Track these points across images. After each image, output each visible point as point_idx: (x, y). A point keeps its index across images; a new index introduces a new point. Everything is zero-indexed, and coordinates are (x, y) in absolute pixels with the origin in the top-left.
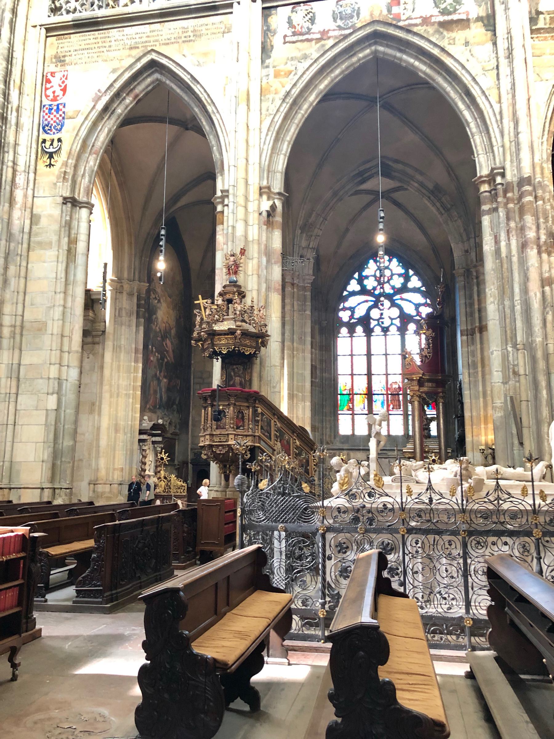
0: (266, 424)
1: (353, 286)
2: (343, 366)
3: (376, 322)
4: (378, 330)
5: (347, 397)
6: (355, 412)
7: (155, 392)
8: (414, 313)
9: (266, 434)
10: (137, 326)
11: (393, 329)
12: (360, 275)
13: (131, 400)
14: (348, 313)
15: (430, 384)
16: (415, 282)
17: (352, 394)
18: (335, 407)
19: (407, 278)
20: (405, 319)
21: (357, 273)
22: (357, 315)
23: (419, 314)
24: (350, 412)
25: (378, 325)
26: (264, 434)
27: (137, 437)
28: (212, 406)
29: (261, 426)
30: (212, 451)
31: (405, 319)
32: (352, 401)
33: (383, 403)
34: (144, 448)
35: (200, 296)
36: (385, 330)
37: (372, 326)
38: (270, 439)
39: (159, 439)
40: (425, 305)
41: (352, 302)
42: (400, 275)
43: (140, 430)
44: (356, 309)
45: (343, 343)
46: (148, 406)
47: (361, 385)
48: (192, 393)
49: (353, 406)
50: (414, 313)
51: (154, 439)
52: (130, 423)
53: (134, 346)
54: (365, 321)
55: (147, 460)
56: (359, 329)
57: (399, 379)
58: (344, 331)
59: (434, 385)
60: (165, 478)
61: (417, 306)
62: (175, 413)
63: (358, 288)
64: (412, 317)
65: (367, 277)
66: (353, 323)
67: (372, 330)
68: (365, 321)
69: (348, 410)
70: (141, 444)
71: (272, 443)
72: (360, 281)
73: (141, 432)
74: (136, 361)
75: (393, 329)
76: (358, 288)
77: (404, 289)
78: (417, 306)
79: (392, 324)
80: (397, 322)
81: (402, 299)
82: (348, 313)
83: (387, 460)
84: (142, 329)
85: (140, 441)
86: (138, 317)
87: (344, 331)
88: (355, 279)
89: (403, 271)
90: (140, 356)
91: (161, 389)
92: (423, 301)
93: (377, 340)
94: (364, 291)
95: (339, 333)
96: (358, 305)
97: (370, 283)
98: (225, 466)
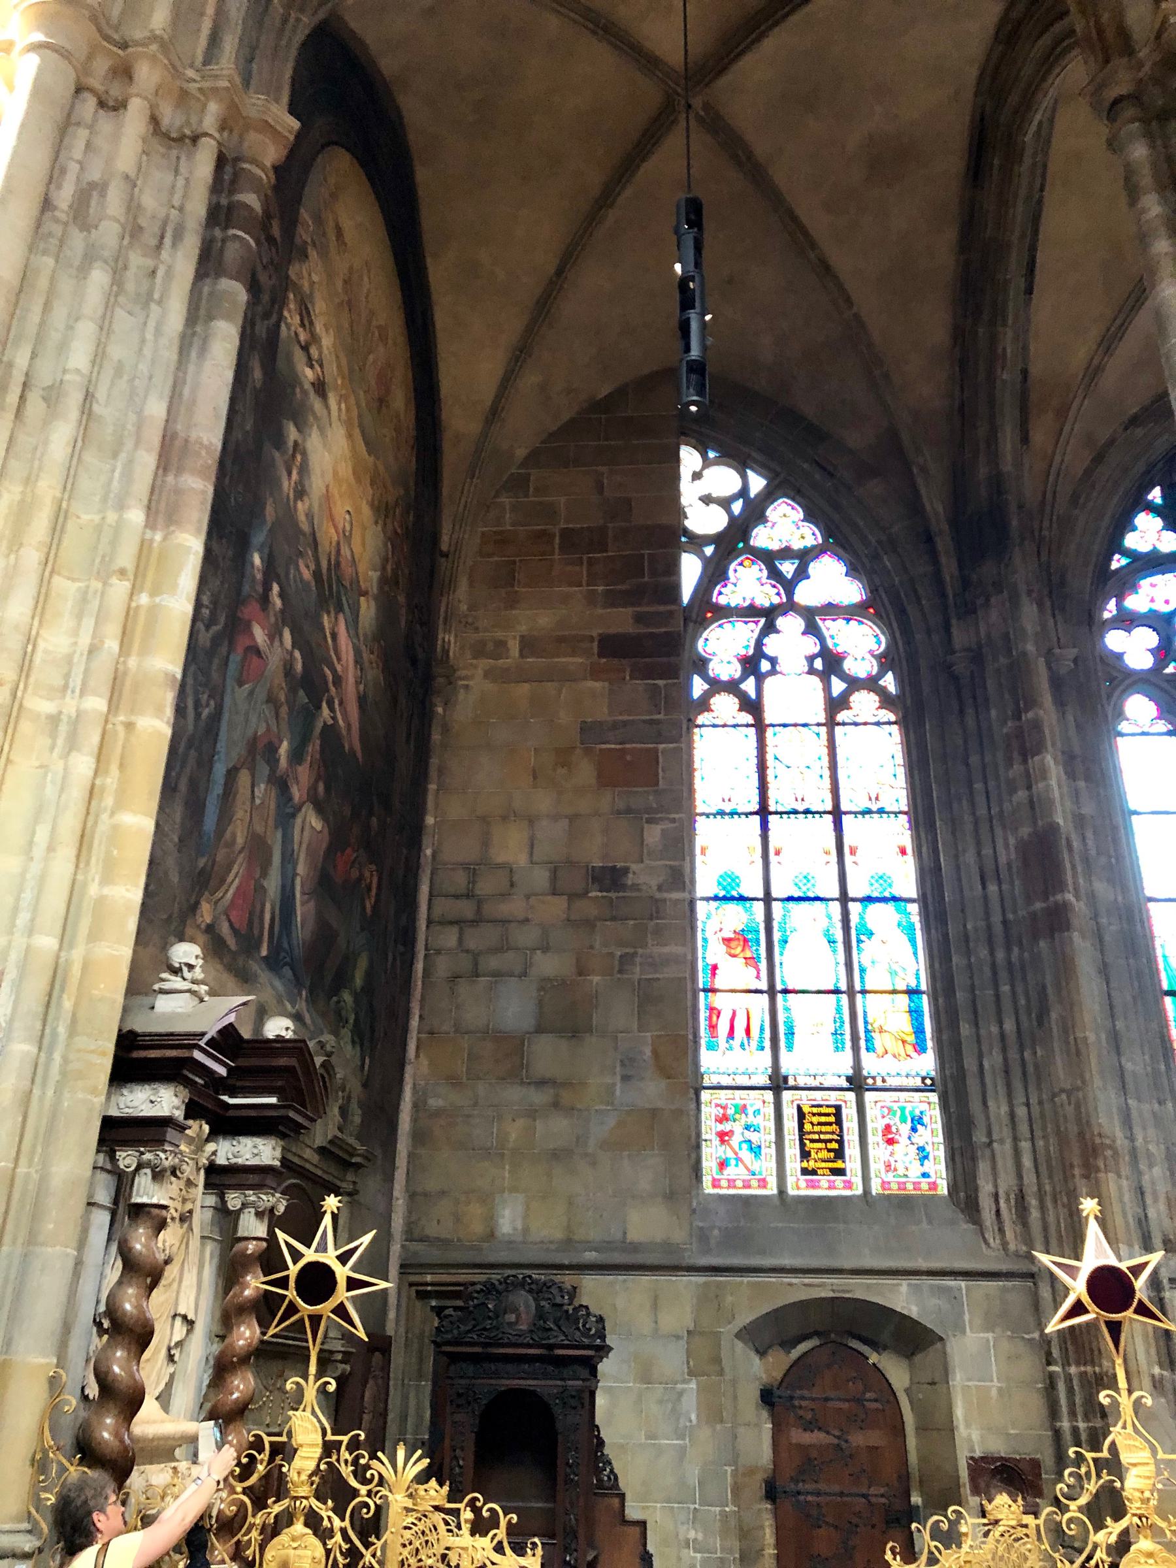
7: (258, 849)
10: (198, 314)
13: (83, 764)
27: (90, 1096)
34: (146, 1192)
39: (259, 1151)
43: (127, 1041)
46: (206, 913)
48: (419, 966)
51: (226, 1151)
52: (47, 942)
53: (157, 409)
55: (158, 1305)
60: (332, 1487)
62: (346, 1033)
70: (127, 1159)
73: (134, 1060)
74: (161, 509)
84: (224, 340)
85: (117, 1132)
86: (209, 263)
90: (198, 488)
91: (289, 858)
95: (1120, 715)
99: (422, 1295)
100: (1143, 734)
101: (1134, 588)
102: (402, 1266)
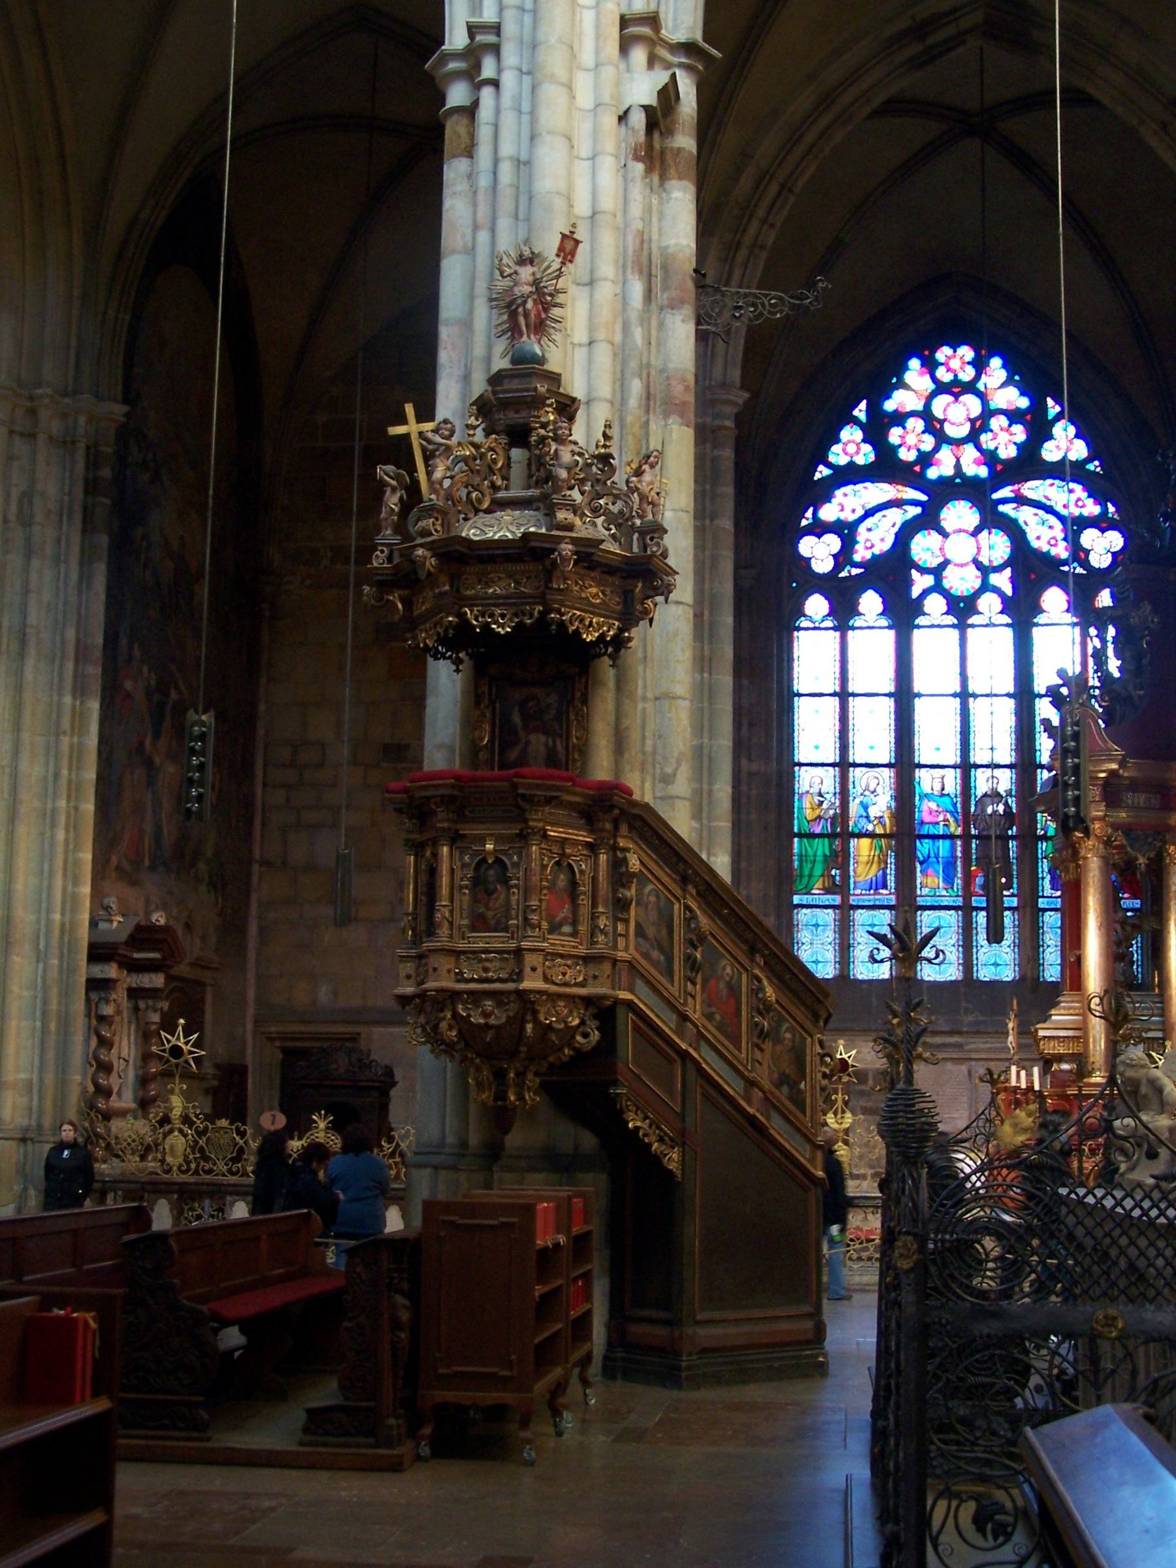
0: (653, 916)
1: (851, 448)
2: (813, 731)
3: (929, 580)
4: (935, 605)
5: (821, 847)
6: (853, 901)
8: (1061, 551)
9: (655, 954)
11: (989, 604)
12: (874, 410)
14: (833, 542)
15: (1141, 799)
16: (1065, 443)
17: (841, 831)
19: (1039, 430)
20: (1031, 571)
21: (863, 405)
22: (861, 554)
23: (1079, 554)
24: (836, 899)
25: (938, 588)
26: (646, 956)
27: (83, 970)
28: (455, 839)
29: (638, 926)
30: (455, 1015)
31: (1031, 571)
32: (840, 859)
33: (950, 865)
34: (108, 1010)
35: (409, 409)
36: (962, 609)
37: (915, 592)
38: (670, 973)
39: (157, 980)
40: (1101, 523)
41: (845, 503)
42: (1014, 416)
43: (92, 946)
44: (862, 528)
45: (813, 654)
47: (875, 797)
49: (845, 876)
50: (1061, 551)
54: (891, 572)
56: (870, 602)
57: (1005, 781)
58: (817, 606)
59: (1155, 801)
61: (1075, 526)
63: (865, 455)
64: (1059, 562)
65: (899, 418)
66: (850, 577)
67: (917, 608)
68: (891, 572)
69: (828, 891)
71: (674, 990)
72: (877, 429)
73: (98, 953)
75: (989, 604)
76: (865, 455)
77: (1028, 464)
78: (1075, 526)
79: (985, 587)
80: (1003, 580)
81: (1020, 500)
82: (833, 542)
83: (964, 1068)
85: (95, 985)
87: (817, 606)
88: (856, 421)
89: (1024, 403)
92: (1092, 509)
93: (934, 645)
94: (887, 467)
96: (869, 514)
97: (909, 441)
98: (500, 1075)
99: (271, 1039)
100: (815, 628)
101: (828, 498)
102: (256, 1022)
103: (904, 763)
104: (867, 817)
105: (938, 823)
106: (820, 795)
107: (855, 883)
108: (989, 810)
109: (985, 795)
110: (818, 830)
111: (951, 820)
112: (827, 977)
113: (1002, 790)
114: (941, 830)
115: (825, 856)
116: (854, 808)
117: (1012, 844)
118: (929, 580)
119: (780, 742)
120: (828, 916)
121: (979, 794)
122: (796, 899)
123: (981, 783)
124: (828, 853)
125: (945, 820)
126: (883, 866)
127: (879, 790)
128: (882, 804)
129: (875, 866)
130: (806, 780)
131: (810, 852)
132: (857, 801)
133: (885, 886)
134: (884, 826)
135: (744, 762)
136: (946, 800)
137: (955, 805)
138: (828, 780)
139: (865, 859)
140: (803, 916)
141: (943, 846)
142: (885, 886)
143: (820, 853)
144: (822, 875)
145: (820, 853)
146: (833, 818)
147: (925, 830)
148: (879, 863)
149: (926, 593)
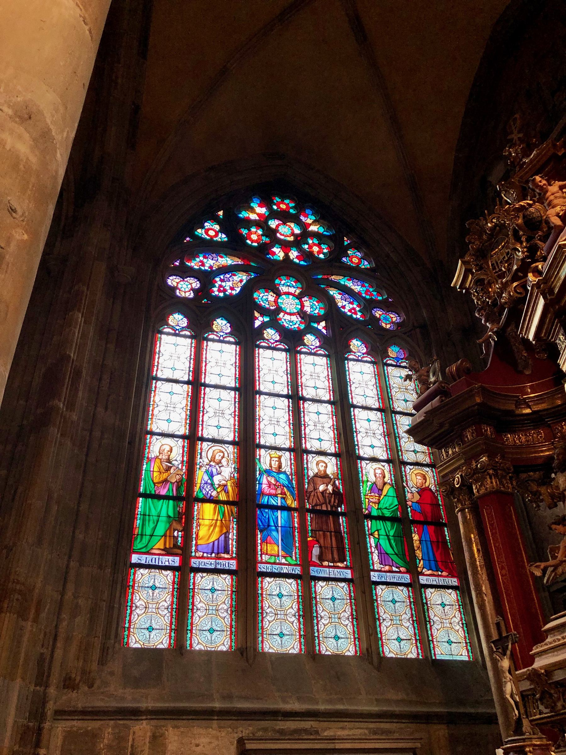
3: (267, 319)
18: (122, 535)
19: (338, 251)
24: (175, 561)
25: (274, 324)
32: (185, 520)
37: (257, 323)
45: (172, 352)
58: (178, 320)
67: (259, 333)
69: (168, 552)
77: (334, 264)
103: (247, 442)
104: (212, 485)
105: (276, 495)
106: (169, 461)
107: (196, 545)
108: (322, 488)
109: (316, 476)
110: (163, 492)
111: (288, 494)
112: (161, 646)
113: (329, 471)
114: (278, 502)
115: (169, 517)
116: (200, 476)
117: (342, 520)
118: (267, 319)
119: (136, 407)
120: (166, 579)
121: (311, 474)
122: (135, 558)
123: (313, 465)
124: (171, 514)
125: (283, 493)
126: (225, 531)
127: (224, 462)
128: (227, 472)
129: (217, 529)
130: (155, 447)
131: (154, 512)
132: (204, 469)
133: (227, 551)
134: (227, 492)
135: (100, 409)
136: (282, 476)
137: (290, 481)
138: (177, 450)
139: (207, 522)
140: (142, 577)
141: (281, 517)
142: (227, 551)
143: (164, 513)
144: (165, 535)
145: (164, 513)
146: (179, 484)
147: (265, 500)
148: (221, 527)
149: (264, 326)
